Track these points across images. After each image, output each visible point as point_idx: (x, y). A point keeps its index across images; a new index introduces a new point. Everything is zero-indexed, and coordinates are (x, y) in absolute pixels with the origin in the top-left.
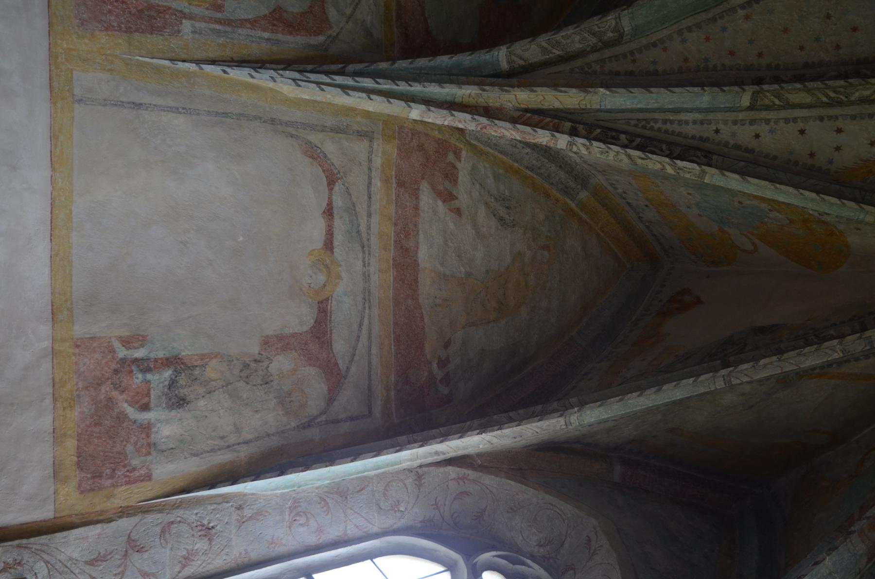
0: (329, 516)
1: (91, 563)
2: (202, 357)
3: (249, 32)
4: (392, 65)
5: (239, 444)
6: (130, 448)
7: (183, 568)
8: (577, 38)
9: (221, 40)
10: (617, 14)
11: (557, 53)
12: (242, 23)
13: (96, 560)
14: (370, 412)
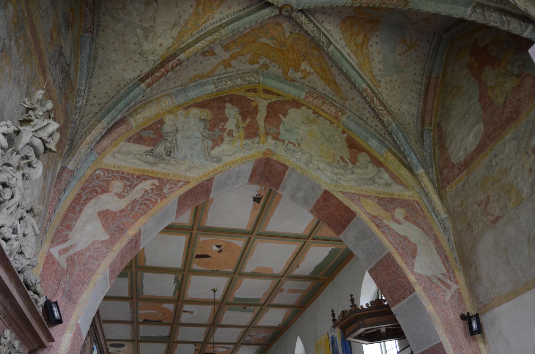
8: (492, 18)
10: (469, 18)
11: (504, 17)
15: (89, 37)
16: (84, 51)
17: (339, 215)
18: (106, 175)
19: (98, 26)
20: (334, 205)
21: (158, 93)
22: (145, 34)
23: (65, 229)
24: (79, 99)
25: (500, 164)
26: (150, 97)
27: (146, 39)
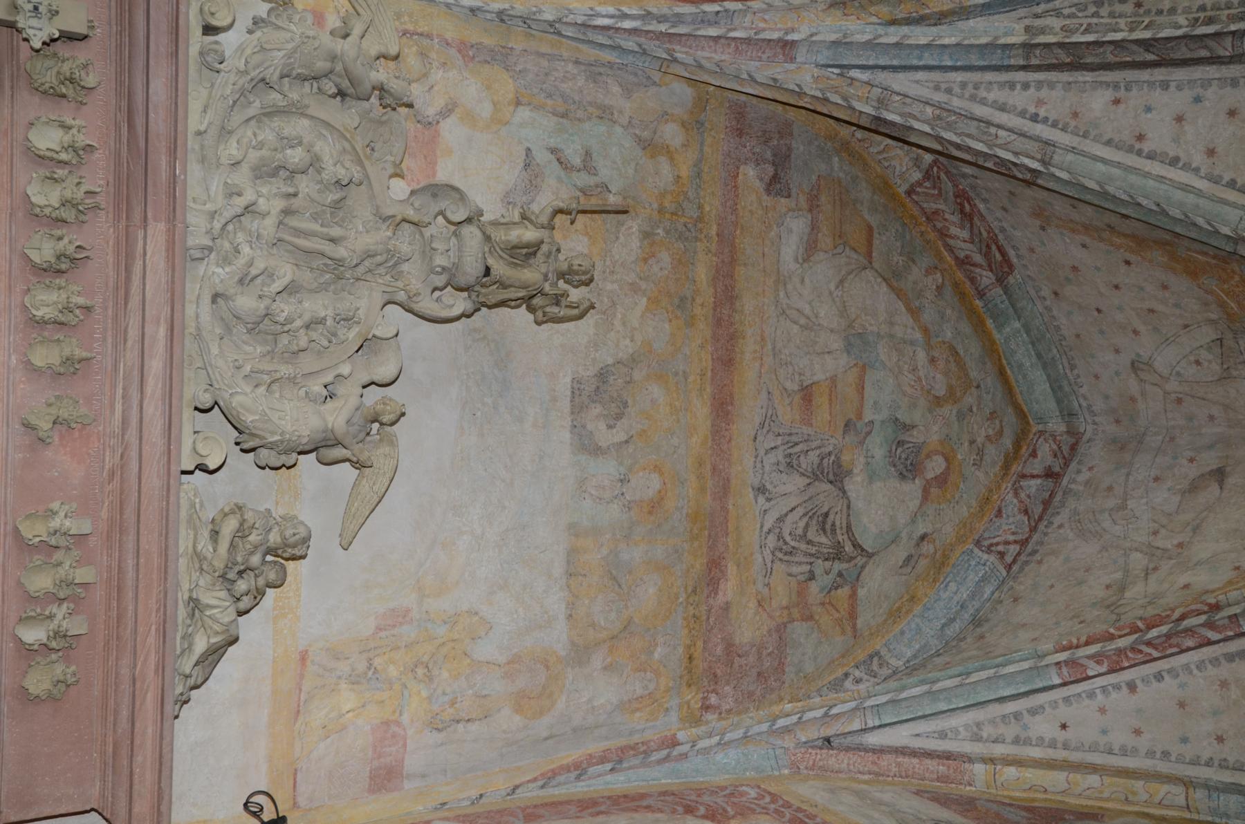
15: (988, 563)
16: (953, 587)
18: (761, 802)
19: (1034, 552)
21: (1135, 751)
22: (1151, 566)
23: (521, 816)
24: (866, 677)
26: (1094, 748)
27: (1147, 574)
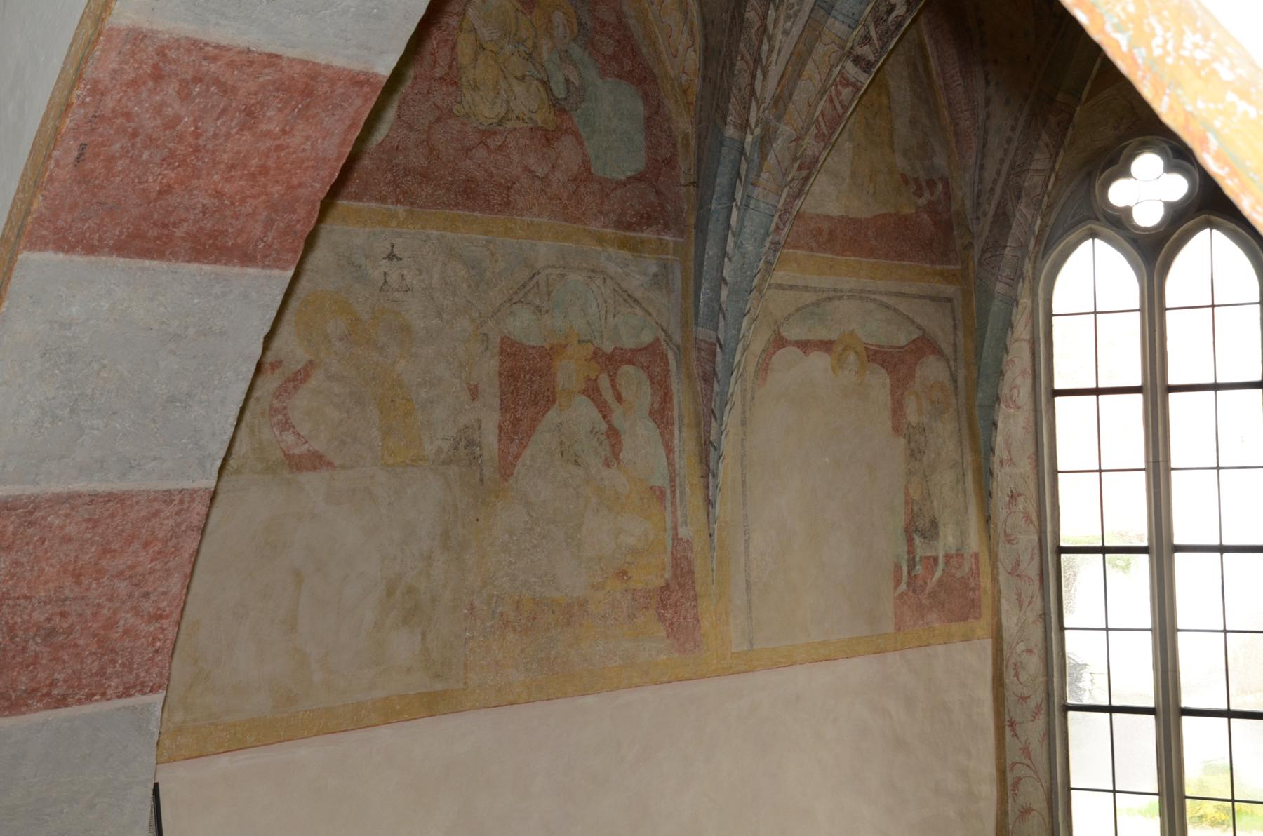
0: (1016, 360)
1: (1021, 606)
2: (907, 503)
3: (677, 454)
4: (726, 283)
5: (963, 463)
6: (959, 575)
7: (1032, 522)
9: (687, 489)
12: (671, 464)
13: (1020, 602)
14: (949, 300)
17: (219, 194)
20: (279, 148)
25: (397, 295)
